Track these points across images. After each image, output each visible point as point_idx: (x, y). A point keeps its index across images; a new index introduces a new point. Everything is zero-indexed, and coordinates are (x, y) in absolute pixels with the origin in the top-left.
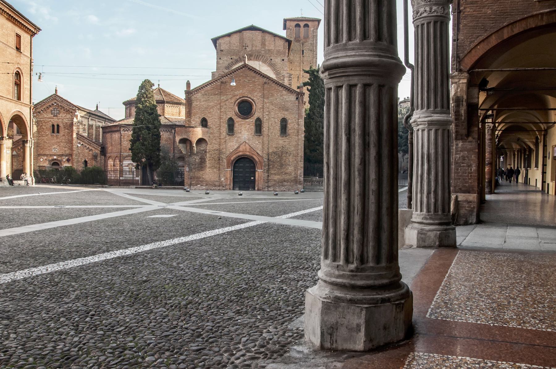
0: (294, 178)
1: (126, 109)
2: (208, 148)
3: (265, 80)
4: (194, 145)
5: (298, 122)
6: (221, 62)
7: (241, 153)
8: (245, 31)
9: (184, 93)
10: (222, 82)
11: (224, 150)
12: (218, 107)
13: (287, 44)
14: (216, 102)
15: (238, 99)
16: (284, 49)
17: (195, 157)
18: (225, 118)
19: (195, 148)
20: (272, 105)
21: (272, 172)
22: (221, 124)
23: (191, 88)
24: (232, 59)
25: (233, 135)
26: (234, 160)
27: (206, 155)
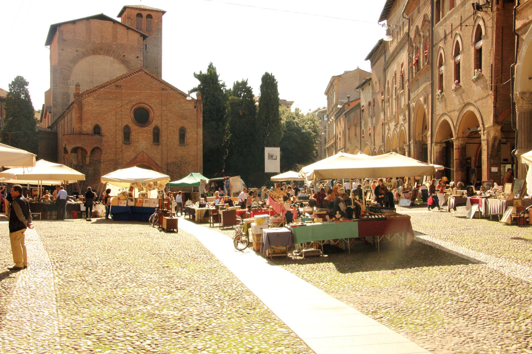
2: (102, 158)
4: (89, 154)
5: (197, 131)
8: (92, 20)
11: (121, 161)
12: (113, 113)
14: (110, 107)
15: (134, 106)
17: (88, 168)
19: (88, 159)
20: (171, 112)
24: (77, 51)
25: (130, 144)
27: (100, 166)
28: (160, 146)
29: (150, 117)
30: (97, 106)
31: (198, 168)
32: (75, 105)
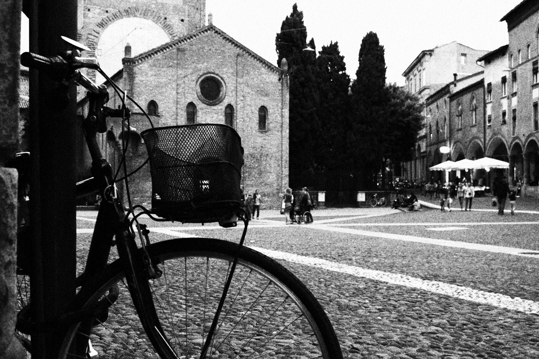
0: (276, 191)
3: (238, 50)
6: (90, 14)
10: (178, 49)
12: (174, 85)
15: (201, 76)
18: (184, 102)
21: (249, 183)
22: (179, 111)
23: (133, 56)
24: (107, 12)
29: (221, 93)
30: (152, 76)
31: (283, 162)
32: (125, 75)
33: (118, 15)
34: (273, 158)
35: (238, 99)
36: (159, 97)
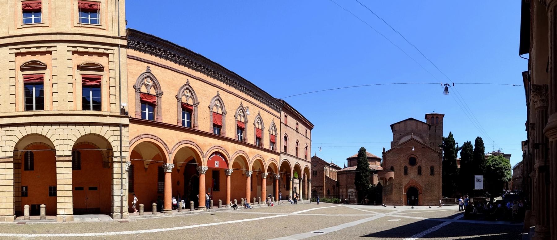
1: (348, 162)
2: (394, 182)
7: (410, 185)
9: (382, 153)
13: (429, 127)
14: (398, 157)
16: (427, 129)
18: (403, 166)
19: (388, 183)
21: (426, 195)
23: (385, 151)
24: (401, 135)
26: (407, 188)
27: (393, 186)
28: (421, 176)
30: (392, 157)
33: (405, 135)
34: (437, 185)
35: (423, 164)
36: (394, 165)
